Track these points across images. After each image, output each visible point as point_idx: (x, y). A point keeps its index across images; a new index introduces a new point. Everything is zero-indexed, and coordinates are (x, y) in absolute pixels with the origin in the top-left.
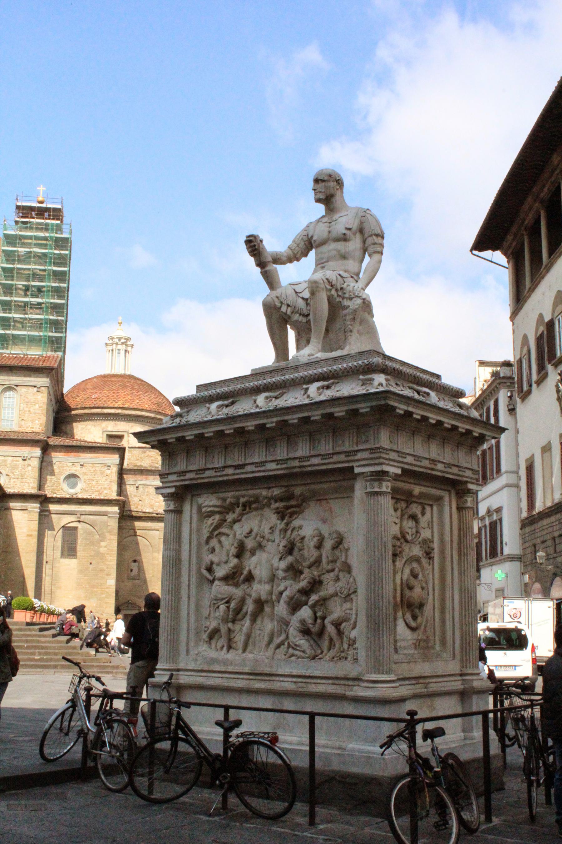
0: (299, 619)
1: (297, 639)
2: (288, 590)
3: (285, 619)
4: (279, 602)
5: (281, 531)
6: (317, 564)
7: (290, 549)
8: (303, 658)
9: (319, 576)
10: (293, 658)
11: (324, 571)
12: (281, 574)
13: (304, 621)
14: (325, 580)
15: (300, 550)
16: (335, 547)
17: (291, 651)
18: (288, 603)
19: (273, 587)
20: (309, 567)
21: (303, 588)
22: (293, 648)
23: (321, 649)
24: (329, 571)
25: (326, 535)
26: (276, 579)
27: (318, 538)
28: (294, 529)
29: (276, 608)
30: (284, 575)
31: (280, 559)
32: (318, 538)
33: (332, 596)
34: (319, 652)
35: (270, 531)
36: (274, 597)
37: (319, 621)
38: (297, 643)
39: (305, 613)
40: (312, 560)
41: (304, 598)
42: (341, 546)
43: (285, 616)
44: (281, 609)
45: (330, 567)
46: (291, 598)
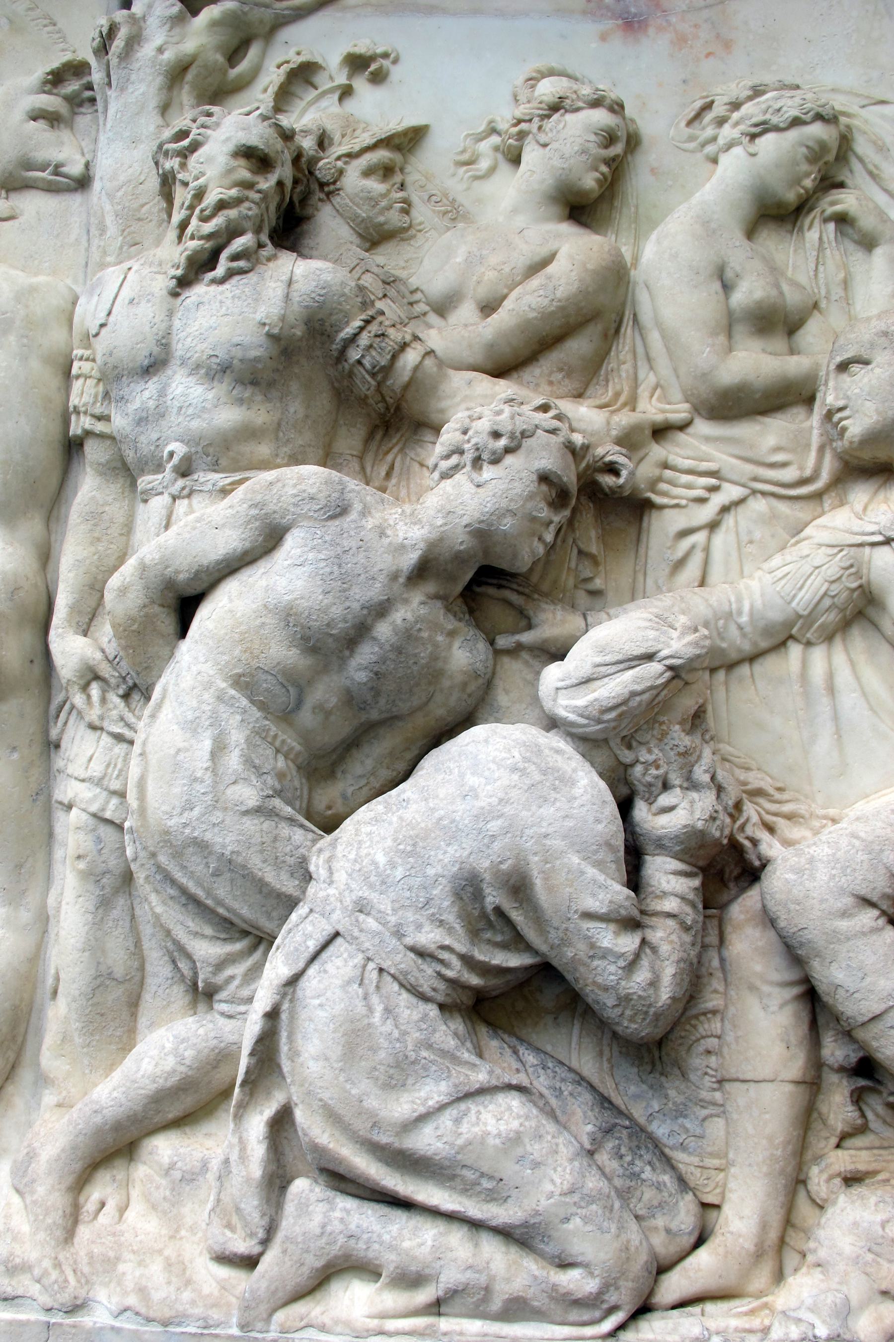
0: (446, 859)
1: (432, 1091)
2: (292, 544)
3: (230, 867)
4: (137, 690)
5: (177, 73)
6: (579, 347)
7: (289, 205)
8: (517, 1309)
9: (629, 441)
10: (354, 1299)
11: (652, 410)
12: (193, 404)
13: (519, 886)
14: (679, 489)
15: (375, 237)
16: (775, 213)
17: (316, 1214)
18: (273, 696)
19: (46, 557)
20: (503, 367)
21: (482, 534)
22: (341, 1180)
23: (683, 1183)
24: (733, 405)
25: (659, 121)
26: (89, 488)
27: (601, 117)
28: (303, 74)
29: (83, 753)
30: (228, 416)
31: (199, 266)
32: (601, 117)
33: (781, 636)
34: (684, 1217)
35: (50, 102)
36: (69, 648)
37: (667, 877)
38: (428, 1141)
39: (506, 788)
40: (526, 303)
41: (463, 654)
42: (845, 201)
43: (231, 836)
44: (180, 748)
45: (754, 362)
46: (327, 644)
